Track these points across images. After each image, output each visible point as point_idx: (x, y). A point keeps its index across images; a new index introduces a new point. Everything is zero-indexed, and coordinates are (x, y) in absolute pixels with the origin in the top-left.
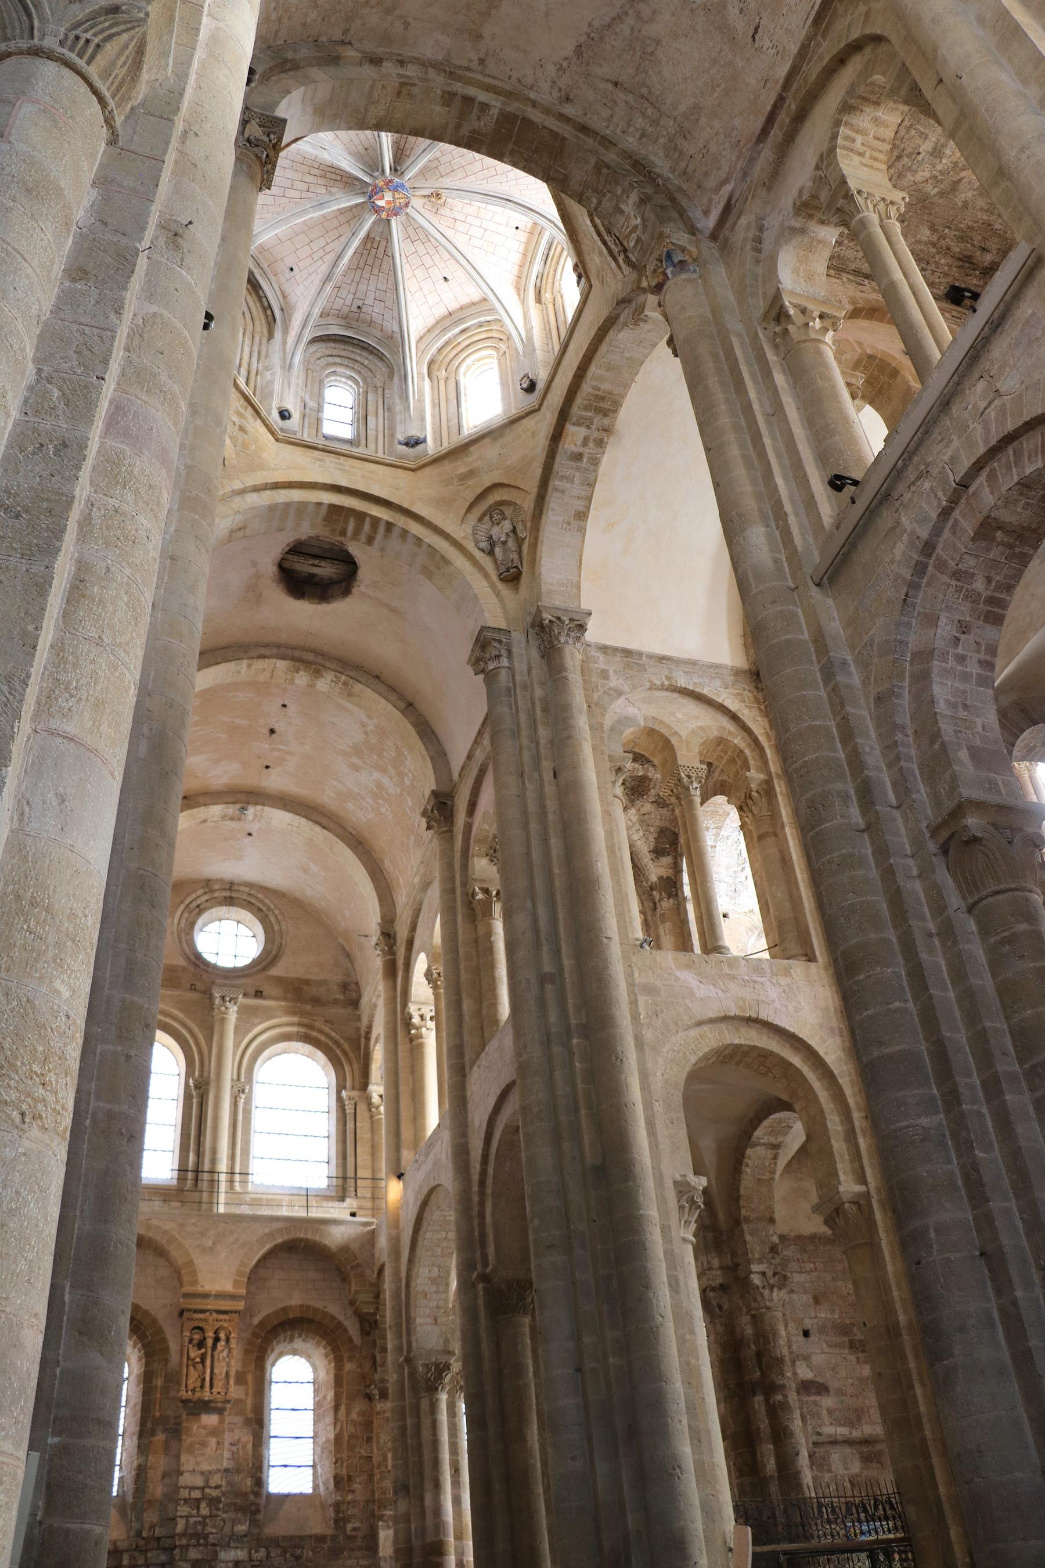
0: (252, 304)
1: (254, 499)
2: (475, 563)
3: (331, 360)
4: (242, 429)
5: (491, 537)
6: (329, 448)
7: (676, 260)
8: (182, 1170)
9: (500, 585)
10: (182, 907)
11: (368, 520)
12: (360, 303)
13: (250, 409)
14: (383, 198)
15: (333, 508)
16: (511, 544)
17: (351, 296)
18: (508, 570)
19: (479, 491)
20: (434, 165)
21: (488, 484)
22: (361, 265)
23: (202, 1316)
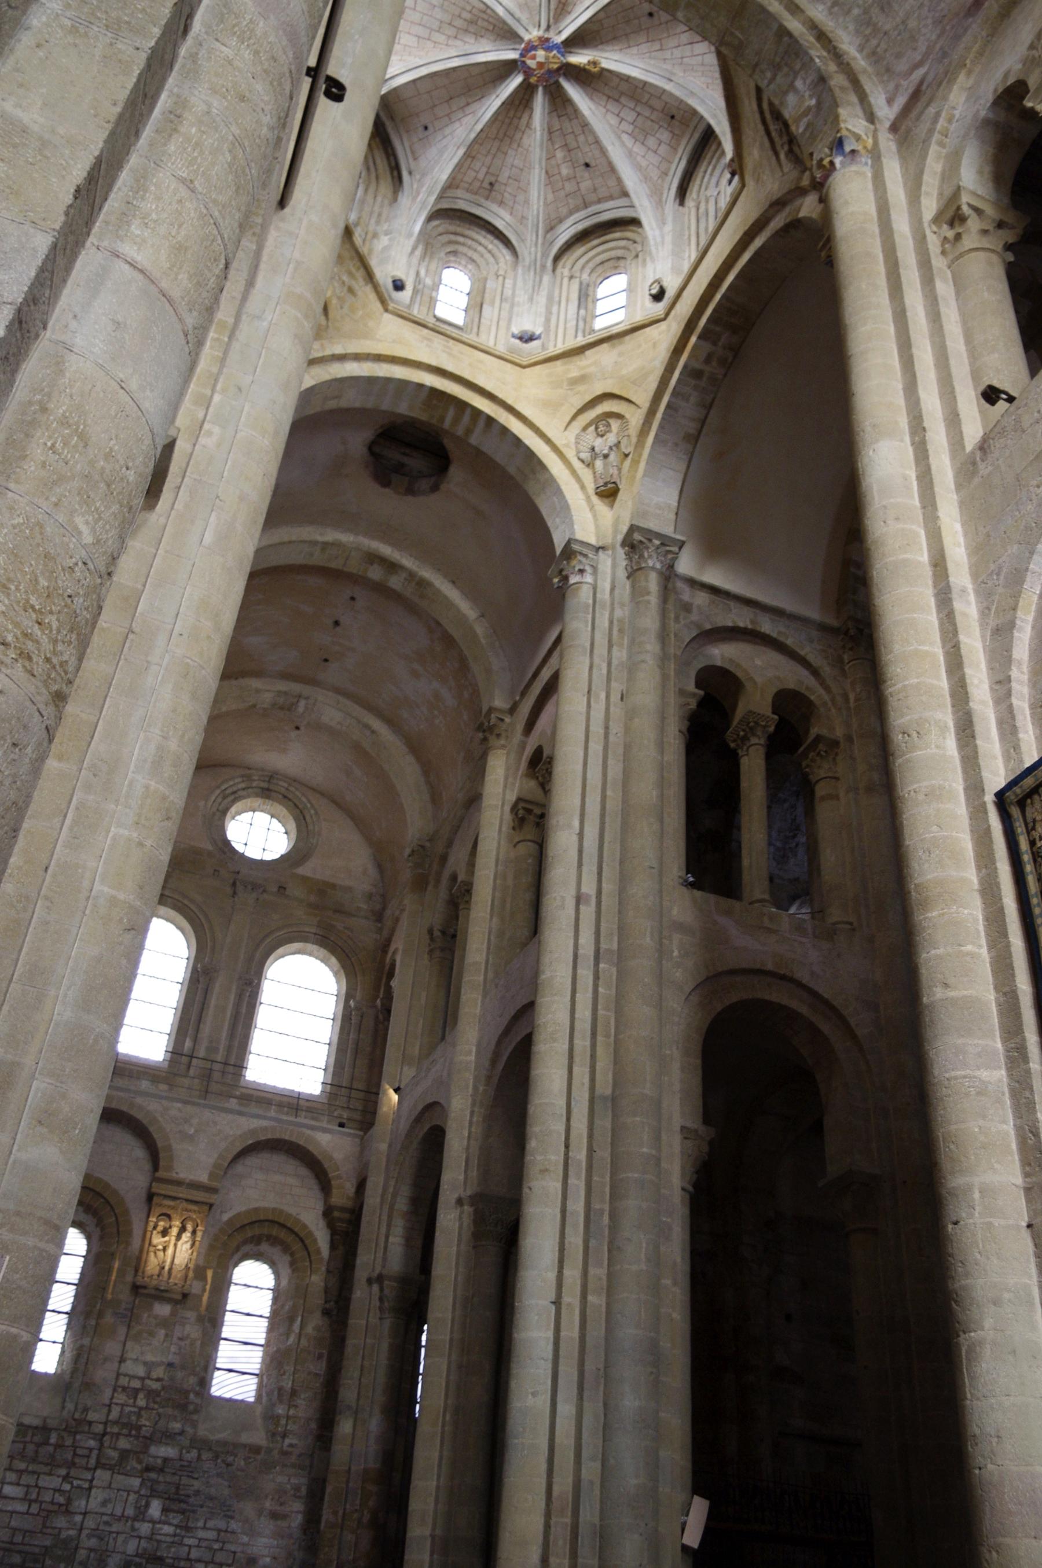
0: (379, 161)
1: (352, 369)
2: (573, 472)
3: (453, 237)
4: (351, 290)
6: (440, 329)
7: (847, 148)
8: (176, 1052)
9: (595, 499)
10: (218, 792)
11: (468, 411)
12: (493, 179)
13: (362, 270)
14: (534, 57)
15: (434, 392)
17: (484, 170)
18: (606, 484)
19: (588, 398)
21: (599, 392)
22: (501, 135)
23: (172, 1203)
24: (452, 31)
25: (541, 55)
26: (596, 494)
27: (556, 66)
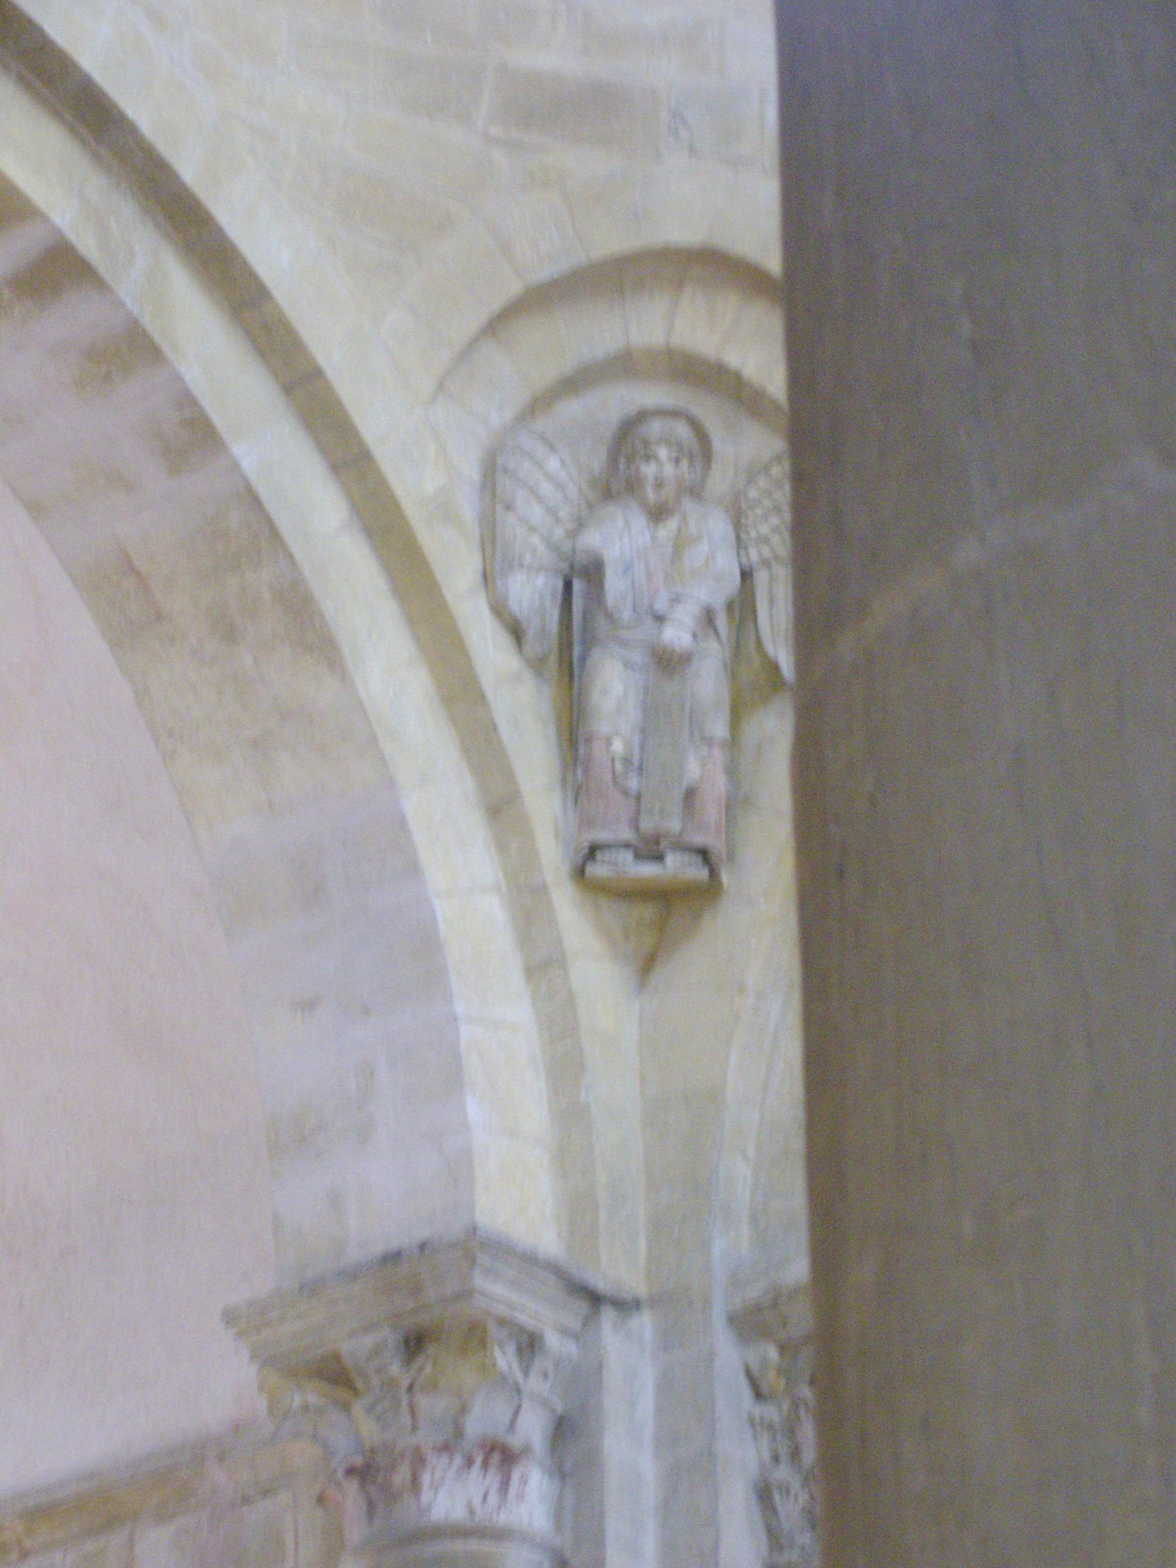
2: (459, 691)
5: (593, 571)
16: (708, 681)
21: (680, 230)
26: (579, 873)
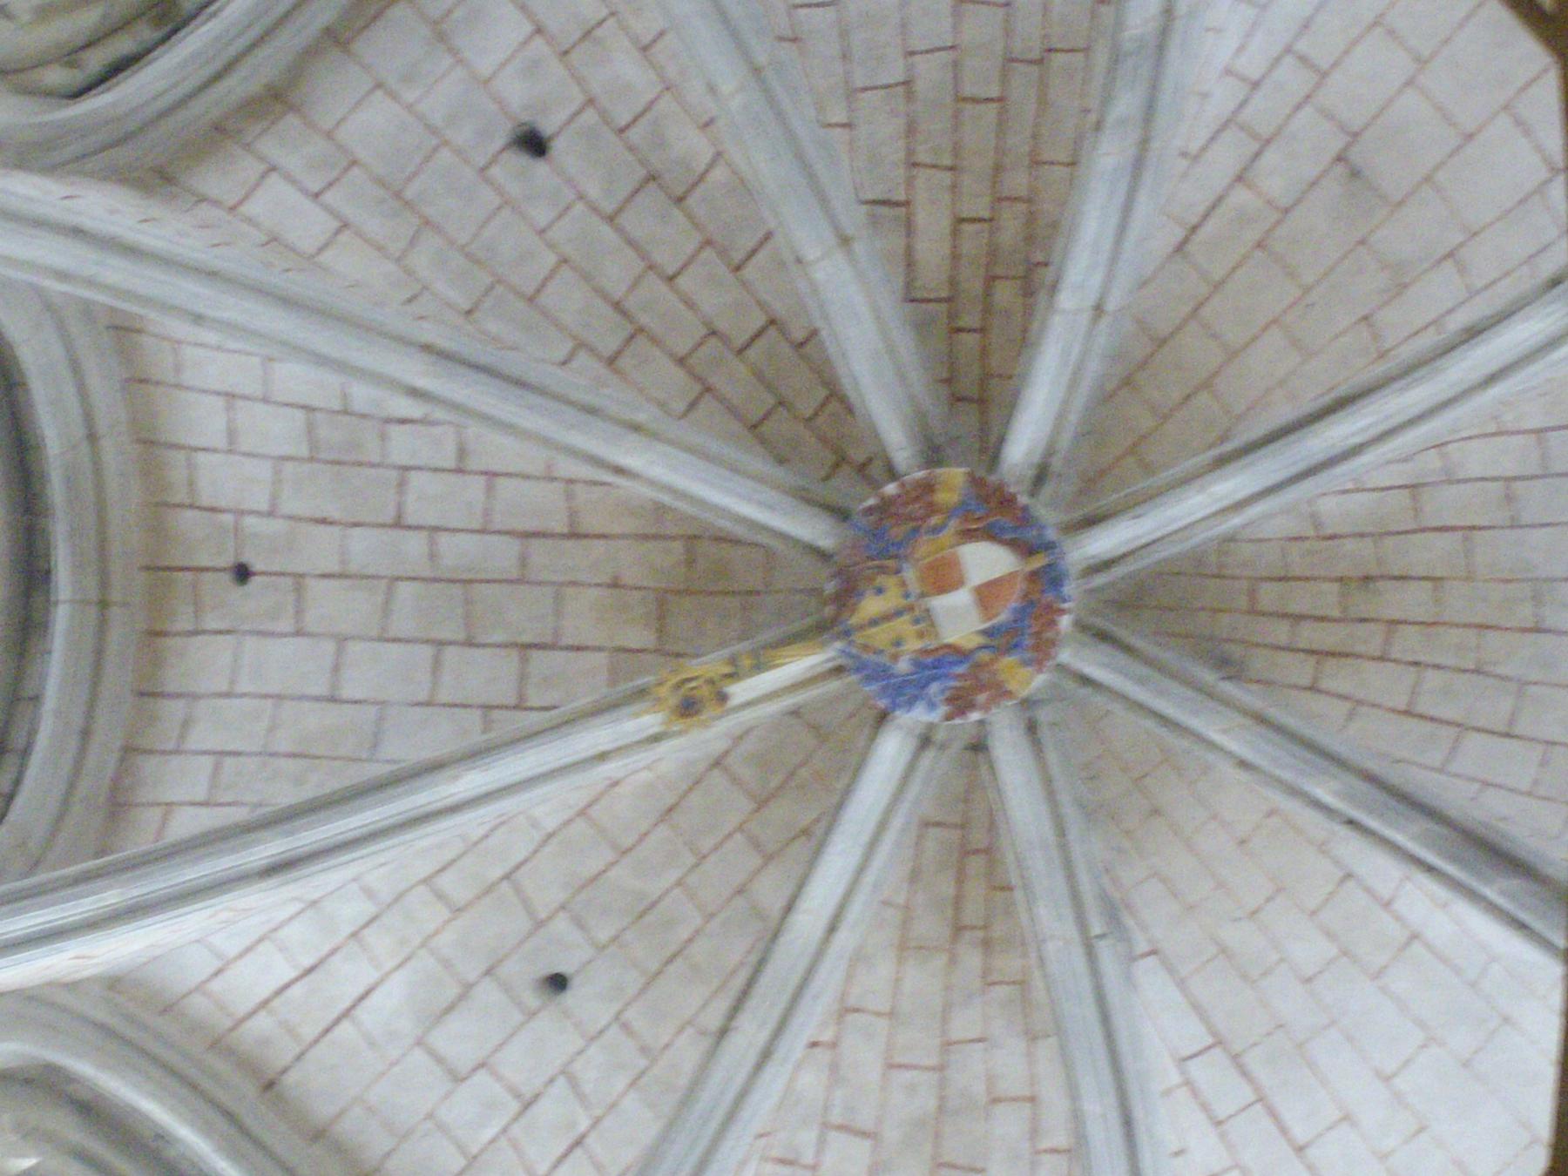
20: (779, 811)
22: (1022, 85)
24: (1445, 505)
25: (958, 618)
27: (871, 606)
